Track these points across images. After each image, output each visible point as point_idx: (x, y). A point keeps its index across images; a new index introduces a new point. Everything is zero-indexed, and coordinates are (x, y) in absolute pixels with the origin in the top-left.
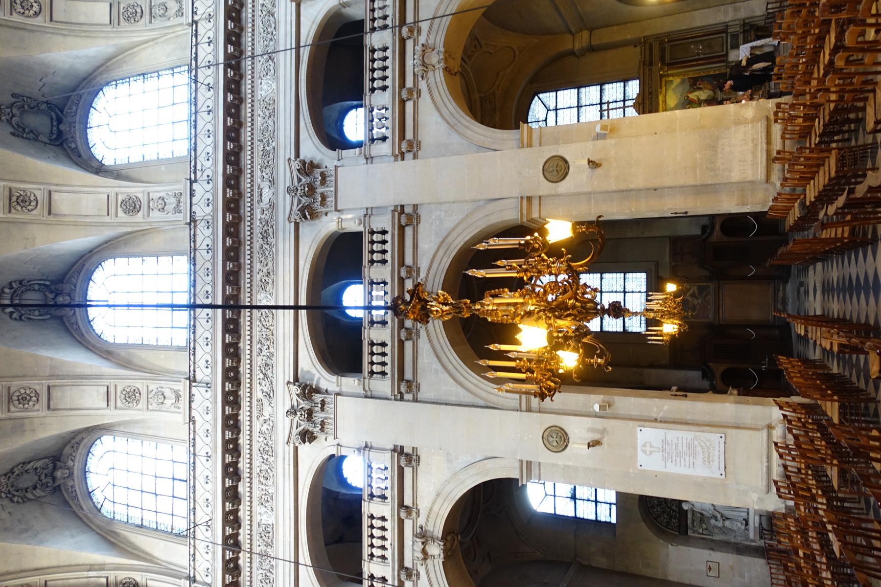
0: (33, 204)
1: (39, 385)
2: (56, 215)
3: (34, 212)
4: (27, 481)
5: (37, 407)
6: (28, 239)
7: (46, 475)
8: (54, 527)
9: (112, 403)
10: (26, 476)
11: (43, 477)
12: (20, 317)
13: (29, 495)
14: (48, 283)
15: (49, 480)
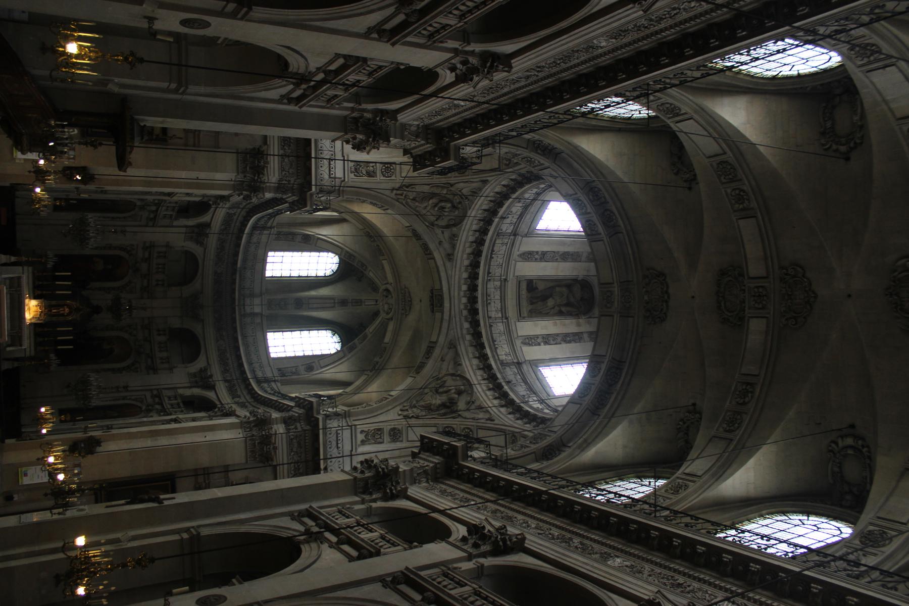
5: (721, 429)
9: (684, 477)
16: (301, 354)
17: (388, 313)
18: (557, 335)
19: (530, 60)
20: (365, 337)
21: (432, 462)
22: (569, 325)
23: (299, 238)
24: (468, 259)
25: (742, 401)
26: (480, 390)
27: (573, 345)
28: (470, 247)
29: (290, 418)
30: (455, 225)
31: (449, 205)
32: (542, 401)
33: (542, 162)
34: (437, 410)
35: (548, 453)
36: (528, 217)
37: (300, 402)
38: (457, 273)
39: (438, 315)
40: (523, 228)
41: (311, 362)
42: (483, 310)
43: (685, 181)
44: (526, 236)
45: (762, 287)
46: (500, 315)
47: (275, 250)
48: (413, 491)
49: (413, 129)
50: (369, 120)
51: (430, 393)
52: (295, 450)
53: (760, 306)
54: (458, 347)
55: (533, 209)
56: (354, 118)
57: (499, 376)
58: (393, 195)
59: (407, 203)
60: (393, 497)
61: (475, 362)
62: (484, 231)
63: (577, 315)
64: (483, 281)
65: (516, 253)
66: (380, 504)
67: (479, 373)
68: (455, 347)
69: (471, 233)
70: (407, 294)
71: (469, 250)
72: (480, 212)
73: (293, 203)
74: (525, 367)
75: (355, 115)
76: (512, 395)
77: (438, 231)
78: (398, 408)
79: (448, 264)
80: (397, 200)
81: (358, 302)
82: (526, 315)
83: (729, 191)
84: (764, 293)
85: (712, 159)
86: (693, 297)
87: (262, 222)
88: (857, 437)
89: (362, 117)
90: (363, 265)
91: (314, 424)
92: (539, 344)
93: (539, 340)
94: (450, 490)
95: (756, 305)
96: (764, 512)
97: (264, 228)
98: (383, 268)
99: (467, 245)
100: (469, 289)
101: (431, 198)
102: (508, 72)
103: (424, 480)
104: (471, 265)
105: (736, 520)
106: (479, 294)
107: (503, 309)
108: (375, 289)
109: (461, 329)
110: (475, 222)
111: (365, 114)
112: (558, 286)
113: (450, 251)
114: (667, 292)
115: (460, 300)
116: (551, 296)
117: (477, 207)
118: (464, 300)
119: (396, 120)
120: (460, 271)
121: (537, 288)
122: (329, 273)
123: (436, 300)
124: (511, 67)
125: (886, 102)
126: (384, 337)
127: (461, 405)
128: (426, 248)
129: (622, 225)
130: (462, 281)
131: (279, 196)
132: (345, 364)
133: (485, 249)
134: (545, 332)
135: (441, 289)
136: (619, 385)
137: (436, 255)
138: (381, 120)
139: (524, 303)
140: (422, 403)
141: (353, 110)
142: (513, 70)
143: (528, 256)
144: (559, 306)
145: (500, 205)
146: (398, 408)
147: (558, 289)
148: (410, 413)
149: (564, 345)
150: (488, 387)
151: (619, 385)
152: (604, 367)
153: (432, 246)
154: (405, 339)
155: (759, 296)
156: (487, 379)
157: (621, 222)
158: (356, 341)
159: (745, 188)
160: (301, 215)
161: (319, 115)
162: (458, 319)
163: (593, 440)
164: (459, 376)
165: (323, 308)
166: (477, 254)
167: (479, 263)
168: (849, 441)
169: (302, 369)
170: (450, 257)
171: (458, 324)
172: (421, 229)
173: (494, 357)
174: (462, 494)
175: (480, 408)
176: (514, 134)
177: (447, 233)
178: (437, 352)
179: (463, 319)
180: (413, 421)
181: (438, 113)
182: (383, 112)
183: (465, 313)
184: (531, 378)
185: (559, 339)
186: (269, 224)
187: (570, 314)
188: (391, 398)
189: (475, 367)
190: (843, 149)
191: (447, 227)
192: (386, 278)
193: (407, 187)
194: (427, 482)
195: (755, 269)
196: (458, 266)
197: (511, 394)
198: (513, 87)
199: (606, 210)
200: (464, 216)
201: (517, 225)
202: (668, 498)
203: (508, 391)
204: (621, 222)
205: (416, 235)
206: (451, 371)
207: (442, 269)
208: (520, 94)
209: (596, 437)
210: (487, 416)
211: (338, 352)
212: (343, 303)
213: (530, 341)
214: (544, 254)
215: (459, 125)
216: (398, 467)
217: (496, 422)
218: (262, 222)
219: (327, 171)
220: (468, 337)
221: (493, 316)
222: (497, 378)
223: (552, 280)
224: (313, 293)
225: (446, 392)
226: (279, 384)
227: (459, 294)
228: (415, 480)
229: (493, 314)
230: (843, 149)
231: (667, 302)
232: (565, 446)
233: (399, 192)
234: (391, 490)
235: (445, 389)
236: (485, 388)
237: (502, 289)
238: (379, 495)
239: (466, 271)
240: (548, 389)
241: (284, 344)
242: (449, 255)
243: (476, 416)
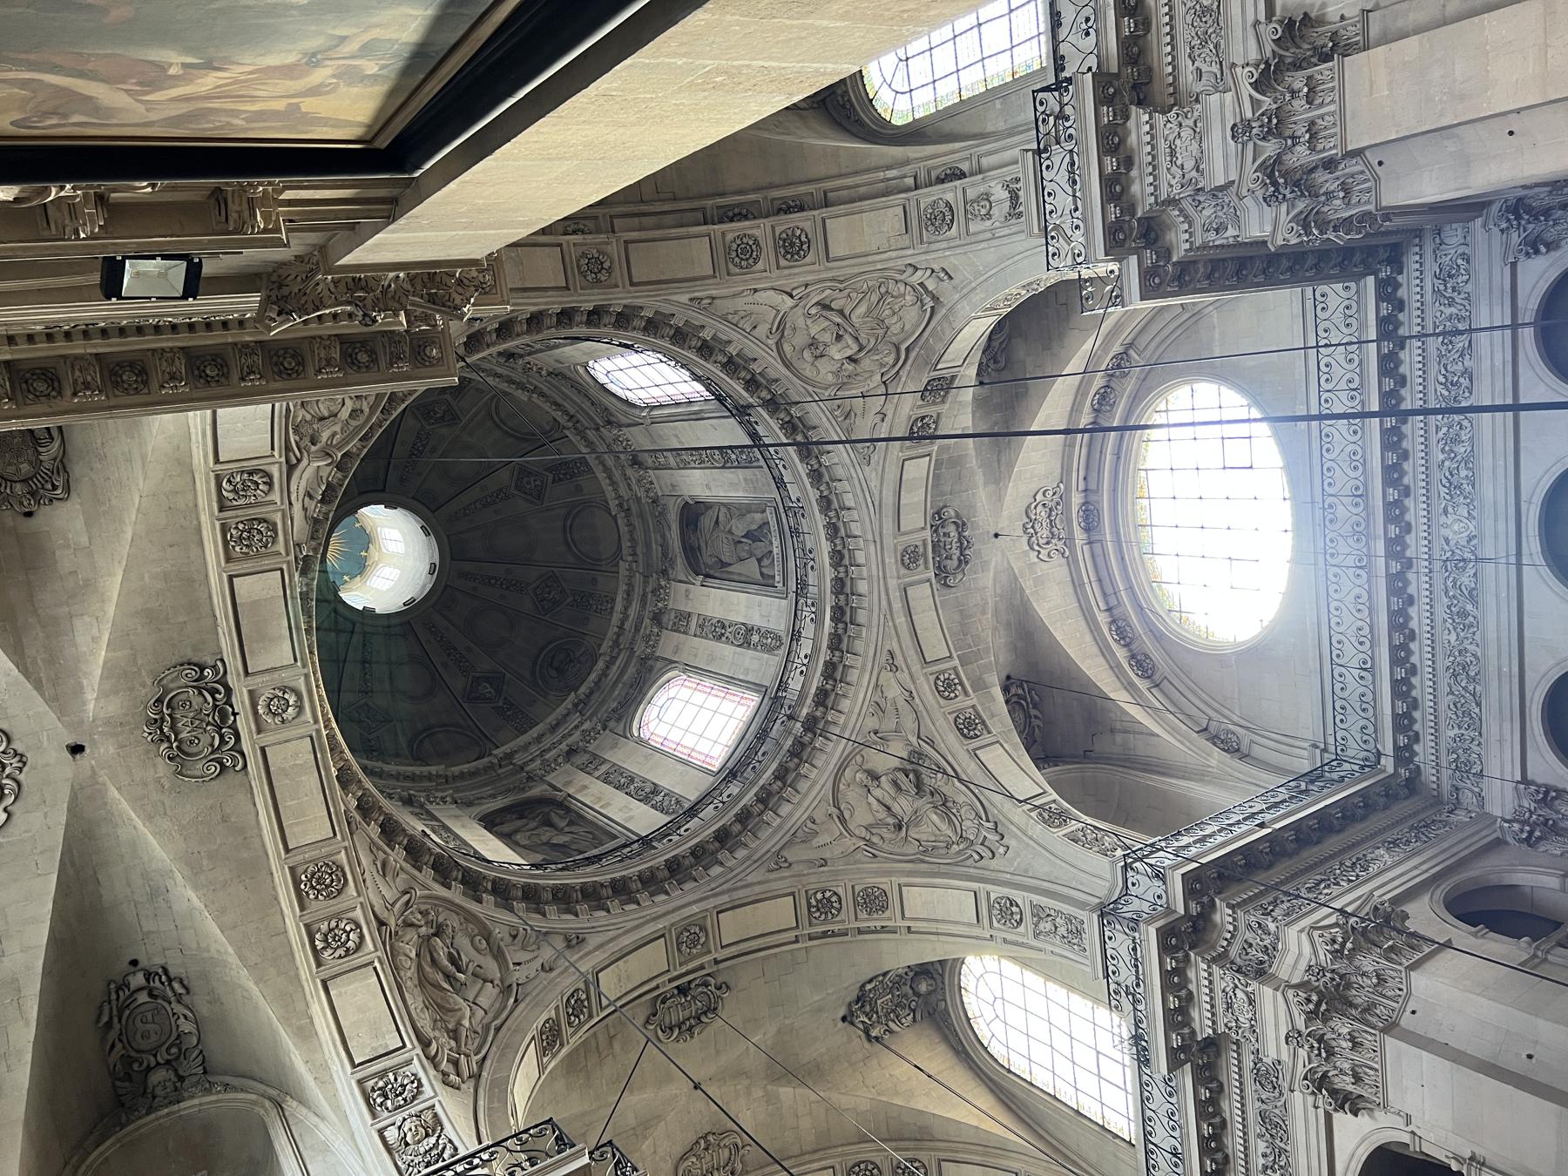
30: (488, 937)
54: (777, 847)
79: (593, 941)
80: (476, 1077)
113: (560, 943)
128: (577, 1006)
146: (994, 864)
153: (568, 983)
191: (499, 955)
193: (429, 1044)
203: (809, 701)
206: (837, 827)
242: (569, 947)
243: (901, 703)
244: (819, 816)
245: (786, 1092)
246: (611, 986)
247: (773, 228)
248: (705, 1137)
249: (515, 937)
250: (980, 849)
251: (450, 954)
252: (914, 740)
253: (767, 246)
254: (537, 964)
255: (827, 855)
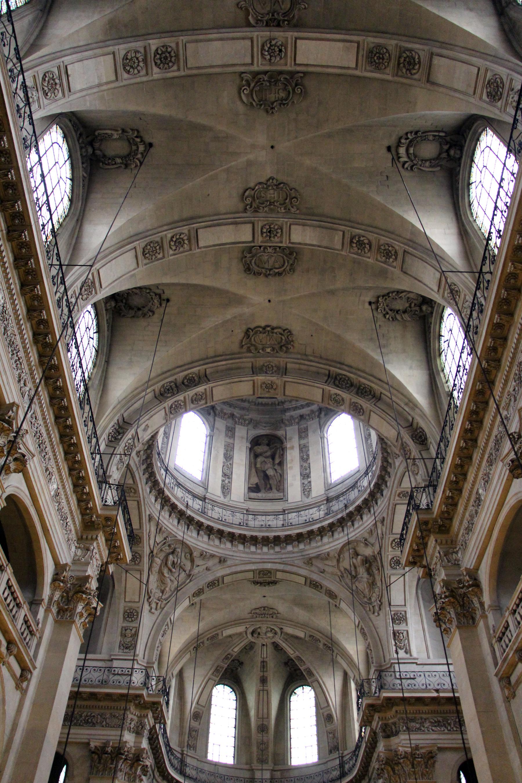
0: (417, 67)
1: (399, 246)
2: (434, 84)
3: (416, 76)
4: (400, 305)
5: (394, 264)
6: (410, 102)
7: (415, 305)
8: (404, 351)
9: (441, 291)
10: (399, 301)
11: (413, 305)
12: (412, 167)
13: (398, 317)
14: (442, 134)
15: (417, 308)
16: (315, 728)
17: (276, 633)
18: (301, 466)
19: (8, 383)
20: (299, 658)
21: (435, 547)
22: (293, 456)
23: (195, 724)
24: (225, 544)
25: (367, 246)
26: (353, 534)
27: (311, 453)
28: (213, 540)
29: (384, 731)
30: (191, 554)
31: (171, 557)
32: (366, 473)
33: (130, 436)
34: (374, 576)
35: (420, 438)
36: (188, 485)
37: (365, 722)
38: (238, 555)
39: (279, 575)
40: (199, 491)
41: (324, 717)
42: (276, 531)
43: (161, 305)
44: (206, 489)
45: (262, 229)
46: (281, 516)
47: (206, 752)
48: (468, 560)
49: (79, 552)
50: (62, 597)
51: (357, 584)
52: (418, 726)
53: (279, 231)
55: (181, 480)
56: (58, 613)
57: (339, 516)
58: (157, 613)
59: (166, 600)
60: (477, 584)
61: (325, 540)
62: (199, 526)
63: (284, 450)
64: (247, 530)
65: (222, 499)
66: (486, 598)
67: (336, 535)
68: (311, 559)
69: (200, 538)
70: (258, 611)
71: (217, 542)
72: (180, 527)
73: (155, 718)
74: (332, 494)
75: (54, 609)
76: (359, 502)
77: (196, 570)
78: (372, 616)
79: (229, 563)
81: (264, 665)
82: (282, 494)
83: (171, 252)
84: (268, 227)
85: (140, 263)
86: (269, 301)
87: (175, 762)
88: (399, 144)
89: (58, 604)
90: (226, 658)
91: (390, 702)
92: (310, 482)
93: (306, 482)
94: (465, 523)
95: (279, 235)
96: (471, 219)
97: (182, 761)
98: (230, 636)
99: (211, 543)
100: (255, 545)
101: (163, 574)
102: (18, 406)
103: (454, 556)
104: (231, 542)
105: (482, 237)
106: (260, 534)
107: (276, 514)
108: (250, 647)
109: (293, 553)
110: (189, 533)
111: (55, 599)
112: (255, 464)
113: (217, 560)
114: (264, 328)
115: (266, 554)
116: (264, 472)
117: (175, 530)
118: (265, 549)
119: (66, 564)
120: (236, 552)
121: (257, 484)
122: (233, 696)
123: (265, 579)
124: (13, 404)
125: (99, 85)
126: (297, 638)
127: (368, 552)
128: (212, 585)
129: (198, 368)
130: (247, 550)
131: (146, 733)
132: (325, 679)
133: (216, 526)
134: (298, 477)
135: (253, 571)
136: (352, 375)
137: (219, 574)
138: (63, 581)
139: (270, 495)
140: (367, 591)
141: (48, 610)
142: (17, 401)
143: (226, 489)
144: (274, 464)
145: (173, 507)
146: (372, 616)
147: (258, 466)
148: (376, 604)
149: (311, 460)
150: (350, 527)
151: (352, 375)
152: (334, 391)
153: (210, 578)
154: (301, 615)
155: (270, 232)
156: (343, 528)
157: (195, 370)
158: (302, 668)
159: (169, 236)
160: (170, 715)
161: (48, 651)
162: (283, 556)
163: (405, 396)
164: (339, 556)
165: (269, 703)
166: (221, 534)
167: (229, 533)
168: (402, 151)
169: (330, 727)
170: (222, 561)
171: (287, 556)
172: (192, 587)
173: (321, 522)
174: (470, 508)
175: (371, 532)
176: (94, 440)
177: (198, 561)
178: (315, 577)
179: (283, 551)
180: (385, 600)
181: (64, 519)
182: (56, 579)
183: (277, 549)
184: (341, 488)
185: (305, 464)
186: (179, 755)
187: (282, 456)
188: (361, 623)
189: (331, 540)
190: (141, 148)
191: (192, 561)
192: (240, 634)
193: (150, 597)
194: (457, 553)
195: (245, 234)
196: (231, 553)
197: (357, 504)
198: (41, 422)
199: (183, 383)
200: (183, 543)
201: (195, 496)
202: (465, 298)
203: (354, 506)
204: (195, 370)
205: (199, 592)
206: (335, 563)
207: (234, 569)
208: (50, 418)
209: (402, 394)
210: (379, 525)
211: (313, 688)
212: (264, 681)
213: (306, 490)
214: (225, 475)
215: (79, 501)
216: (443, 580)
217: (385, 515)
218: (175, 762)
219: (124, 677)
220: (302, 546)
221: (282, 522)
222: (342, 518)
223: (250, 470)
224: (252, 713)
225: (355, 567)
226: (346, 753)
227: (259, 554)
228: (455, 564)
229: (280, 523)
230: (141, 148)
231: (273, 329)
232: (411, 425)
233: (154, 605)
234: (470, 586)
235: (353, 569)
236: (352, 529)
237: (255, 514)
238: (475, 600)
239: (236, 546)
240: (353, 473)
241: (304, 747)
242: (220, 562)
244: (331, 554)
245: (297, 610)
246: (227, 580)
247: (351, 399)
248: (264, 607)
249: (201, 555)
250: (371, 607)
251: (174, 561)
252: (376, 553)
253: (347, 403)
254: (204, 567)
255: (327, 569)
